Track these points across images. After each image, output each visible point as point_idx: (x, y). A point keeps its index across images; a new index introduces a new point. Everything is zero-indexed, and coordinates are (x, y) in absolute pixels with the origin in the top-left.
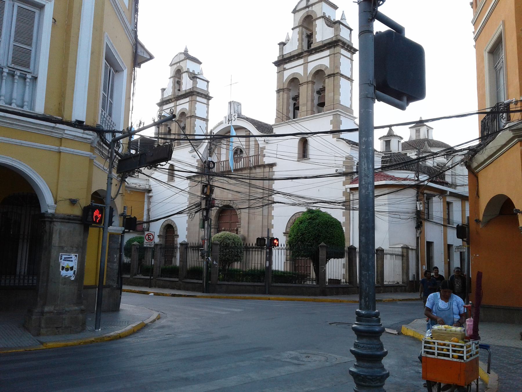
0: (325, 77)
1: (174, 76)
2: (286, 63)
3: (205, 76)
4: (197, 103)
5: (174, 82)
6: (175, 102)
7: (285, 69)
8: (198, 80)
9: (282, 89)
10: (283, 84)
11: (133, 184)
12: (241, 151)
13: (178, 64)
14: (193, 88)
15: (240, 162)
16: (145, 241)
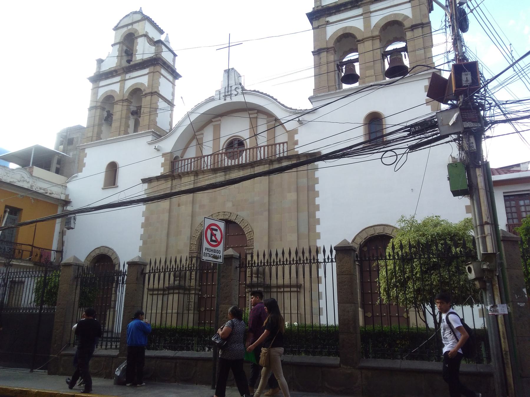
0: (405, 29)
1: (122, 42)
2: (330, 15)
3: (172, 46)
4: (162, 76)
5: (122, 50)
6: (124, 75)
7: (328, 23)
8: (163, 47)
9: (324, 49)
10: (326, 42)
11: (40, 188)
12: (241, 143)
13: (130, 27)
14: (156, 55)
15: (241, 158)
16: (206, 245)
